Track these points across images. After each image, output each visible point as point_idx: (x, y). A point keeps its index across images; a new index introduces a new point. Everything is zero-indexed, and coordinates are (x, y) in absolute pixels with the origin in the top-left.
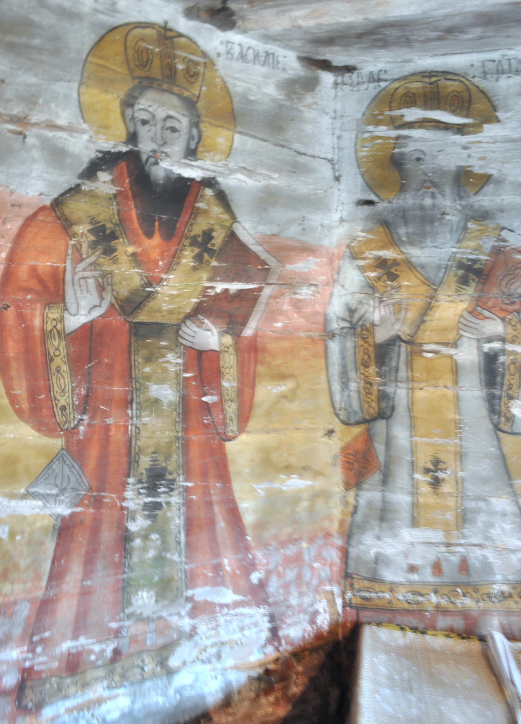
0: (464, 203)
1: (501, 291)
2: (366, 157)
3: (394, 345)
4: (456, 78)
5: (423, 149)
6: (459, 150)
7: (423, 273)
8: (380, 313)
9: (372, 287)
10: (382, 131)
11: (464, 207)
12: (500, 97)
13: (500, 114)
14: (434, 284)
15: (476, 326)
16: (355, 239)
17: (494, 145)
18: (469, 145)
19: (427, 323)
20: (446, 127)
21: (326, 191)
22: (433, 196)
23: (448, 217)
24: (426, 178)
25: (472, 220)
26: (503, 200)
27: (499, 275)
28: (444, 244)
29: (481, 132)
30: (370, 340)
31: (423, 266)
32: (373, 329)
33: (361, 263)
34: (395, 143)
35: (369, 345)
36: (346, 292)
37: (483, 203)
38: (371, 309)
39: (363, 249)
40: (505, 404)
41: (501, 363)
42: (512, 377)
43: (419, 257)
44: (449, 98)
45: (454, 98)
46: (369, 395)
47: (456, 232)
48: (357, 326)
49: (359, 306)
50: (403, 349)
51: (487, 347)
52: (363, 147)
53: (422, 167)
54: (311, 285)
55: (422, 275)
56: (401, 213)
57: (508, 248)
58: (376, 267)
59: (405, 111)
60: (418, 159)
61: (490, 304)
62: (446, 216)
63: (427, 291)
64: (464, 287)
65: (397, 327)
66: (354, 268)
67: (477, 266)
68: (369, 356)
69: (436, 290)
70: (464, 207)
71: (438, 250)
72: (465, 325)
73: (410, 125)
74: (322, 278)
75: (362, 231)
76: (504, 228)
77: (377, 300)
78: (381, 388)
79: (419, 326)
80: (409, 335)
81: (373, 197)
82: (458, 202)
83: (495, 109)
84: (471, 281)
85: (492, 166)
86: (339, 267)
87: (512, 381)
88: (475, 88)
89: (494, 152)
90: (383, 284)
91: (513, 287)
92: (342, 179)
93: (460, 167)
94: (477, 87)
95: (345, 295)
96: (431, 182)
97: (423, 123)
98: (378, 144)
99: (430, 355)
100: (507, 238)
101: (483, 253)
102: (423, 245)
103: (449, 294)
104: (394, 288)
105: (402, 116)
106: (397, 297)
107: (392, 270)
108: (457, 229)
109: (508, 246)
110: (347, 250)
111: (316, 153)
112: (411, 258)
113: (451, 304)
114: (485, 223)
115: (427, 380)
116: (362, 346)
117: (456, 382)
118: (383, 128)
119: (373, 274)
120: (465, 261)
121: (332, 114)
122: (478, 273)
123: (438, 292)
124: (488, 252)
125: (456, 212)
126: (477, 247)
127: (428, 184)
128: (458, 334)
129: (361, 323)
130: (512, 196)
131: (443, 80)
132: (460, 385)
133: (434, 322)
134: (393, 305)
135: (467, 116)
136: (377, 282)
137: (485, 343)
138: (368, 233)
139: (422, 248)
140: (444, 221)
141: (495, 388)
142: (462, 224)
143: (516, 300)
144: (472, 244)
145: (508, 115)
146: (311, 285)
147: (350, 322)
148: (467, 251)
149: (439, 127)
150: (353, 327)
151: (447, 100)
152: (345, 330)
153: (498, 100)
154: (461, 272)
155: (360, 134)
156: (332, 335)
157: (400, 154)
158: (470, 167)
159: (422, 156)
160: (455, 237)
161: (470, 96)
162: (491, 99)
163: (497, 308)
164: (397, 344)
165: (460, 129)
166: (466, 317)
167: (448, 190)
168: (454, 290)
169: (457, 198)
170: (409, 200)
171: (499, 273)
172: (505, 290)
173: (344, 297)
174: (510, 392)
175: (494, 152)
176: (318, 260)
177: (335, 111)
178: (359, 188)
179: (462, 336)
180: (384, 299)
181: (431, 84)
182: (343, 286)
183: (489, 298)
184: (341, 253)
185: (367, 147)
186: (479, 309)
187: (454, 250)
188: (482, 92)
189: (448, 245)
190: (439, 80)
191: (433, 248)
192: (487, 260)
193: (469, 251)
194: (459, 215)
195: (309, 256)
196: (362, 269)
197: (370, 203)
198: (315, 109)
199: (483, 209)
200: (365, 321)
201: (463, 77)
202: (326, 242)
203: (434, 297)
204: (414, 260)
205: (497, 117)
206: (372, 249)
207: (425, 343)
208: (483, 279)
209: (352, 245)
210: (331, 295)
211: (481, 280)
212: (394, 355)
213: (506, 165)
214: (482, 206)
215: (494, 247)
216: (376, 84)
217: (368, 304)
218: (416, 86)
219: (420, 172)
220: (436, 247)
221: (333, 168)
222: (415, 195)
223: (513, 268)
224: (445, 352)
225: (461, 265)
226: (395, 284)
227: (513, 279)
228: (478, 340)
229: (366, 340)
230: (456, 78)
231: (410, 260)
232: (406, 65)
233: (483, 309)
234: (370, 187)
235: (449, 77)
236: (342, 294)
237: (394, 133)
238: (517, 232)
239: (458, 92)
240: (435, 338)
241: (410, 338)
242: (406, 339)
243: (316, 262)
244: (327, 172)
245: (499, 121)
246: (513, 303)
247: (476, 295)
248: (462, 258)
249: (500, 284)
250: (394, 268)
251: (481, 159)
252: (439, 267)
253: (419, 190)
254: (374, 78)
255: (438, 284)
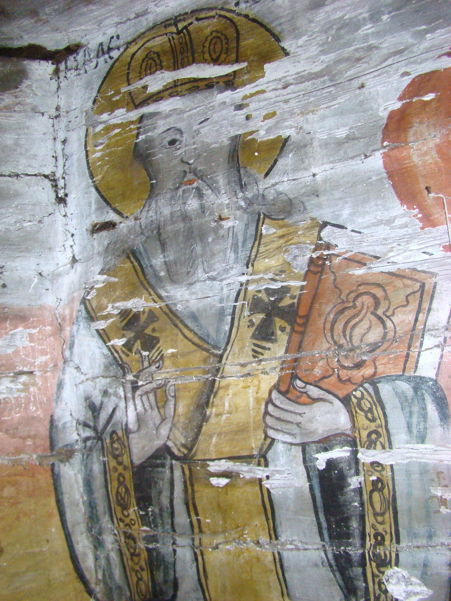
0: (249, 195)
1: (335, 343)
2: (99, 159)
3: (163, 466)
4: (213, 13)
5: (178, 126)
6: (231, 111)
7: (196, 329)
8: (136, 409)
9: (123, 367)
10: (121, 115)
11: (250, 203)
12: (283, 20)
13: (285, 44)
14: (216, 347)
15: (299, 419)
16: (92, 288)
17: (285, 92)
18: (246, 102)
19: (213, 420)
20: (208, 85)
21: (40, 222)
22: (200, 195)
23: (227, 224)
24: (186, 168)
25: (267, 220)
26: (314, 175)
27: (329, 314)
28: (226, 271)
29: (263, 77)
30: (126, 460)
31: (194, 317)
32: (128, 438)
33: (102, 325)
34: (139, 128)
35: (125, 468)
36: (83, 378)
37: (280, 188)
38: (122, 404)
39: (104, 301)
40: (374, 575)
41: (354, 490)
42: (380, 519)
43: (187, 301)
44: (207, 44)
45: (214, 41)
46: (136, 559)
47: (243, 246)
48: (104, 435)
49: (106, 400)
50: (178, 474)
51: (321, 460)
52: (96, 146)
53: (179, 152)
54: (22, 373)
55: (196, 334)
56: (155, 232)
57: (337, 261)
58: (123, 329)
59: (147, 80)
60: (172, 142)
61: (318, 372)
62: (223, 223)
63: (205, 361)
64: (269, 345)
65: (164, 431)
66: (93, 336)
67: (286, 302)
68: (127, 489)
69: (221, 357)
70: (250, 203)
71: (216, 284)
72: (278, 419)
73: (157, 97)
74: (41, 359)
75: (102, 272)
76: (325, 224)
77: (129, 386)
78: (150, 546)
79: (200, 427)
80: (184, 446)
81: (112, 216)
82: (240, 195)
83: (278, 40)
84: (279, 332)
85: (286, 124)
86: (72, 336)
87: (380, 528)
88: (243, 18)
89: (286, 102)
90: (137, 356)
91: (358, 332)
92: (69, 200)
93: (235, 139)
94: (246, 16)
95: (83, 382)
96: (194, 172)
97: (173, 90)
98: (116, 135)
99: (224, 481)
100: (333, 242)
101: (296, 278)
102: (191, 280)
103: (242, 361)
104: (155, 362)
105: (145, 87)
106: (160, 377)
107: (148, 331)
108: (245, 241)
109: (338, 256)
110: (83, 307)
111: (20, 169)
112: (175, 305)
113: (250, 379)
114: (288, 221)
115: (224, 532)
116: (116, 469)
117: (274, 534)
118: (121, 112)
119: (119, 342)
120: (263, 296)
121: (53, 113)
122: (291, 314)
123: (224, 361)
124: (303, 272)
125: (238, 213)
126: (281, 267)
127: (190, 176)
128: (266, 436)
129: (109, 429)
130: (327, 167)
131: (195, 23)
132: (282, 539)
133: (224, 417)
134: (154, 390)
135: (237, 61)
136: (128, 356)
137: (318, 452)
138: (109, 275)
139: (191, 284)
140: (222, 232)
141: (350, 544)
142: (252, 230)
143: (364, 358)
144: (273, 262)
145: (300, 42)
146: (22, 373)
147: (95, 429)
148: (265, 277)
149: (198, 87)
150: (99, 437)
151: (204, 47)
152: (89, 443)
153: (280, 24)
154: (258, 318)
155: (91, 130)
156: (68, 454)
157: (146, 141)
158: (252, 133)
159: (178, 137)
160: (243, 255)
161: (237, 31)
162: (269, 27)
163: (333, 379)
164: (168, 462)
165: (230, 83)
166: (278, 403)
167: (221, 180)
168: (251, 353)
169: (237, 188)
170: (162, 208)
171: (327, 308)
172: (342, 341)
173: (81, 387)
174: (380, 550)
175: (286, 102)
176: (34, 331)
177: (58, 109)
178: (94, 207)
179: (273, 440)
180: (140, 383)
181: (179, 32)
182: (78, 368)
183: (314, 363)
184: (75, 313)
185: (102, 144)
186: (299, 383)
187: (244, 279)
188: (254, 20)
189: (232, 272)
190: (191, 23)
191: (208, 282)
192: (302, 288)
193: (271, 276)
194: (246, 216)
195: (16, 327)
196: (104, 336)
197: (109, 226)
198: (20, 112)
199: (283, 197)
200: (116, 424)
201: (222, 9)
202: (49, 300)
203: (218, 370)
204: (179, 307)
205: (283, 49)
206: (115, 301)
207: (213, 460)
208: (299, 325)
209: (89, 297)
210: (60, 386)
211: (297, 328)
212: (164, 485)
213: (310, 116)
214: (279, 194)
215: (311, 261)
216: (107, 56)
217: (116, 394)
218: (159, 42)
219: (176, 162)
220: (213, 279)
221: (55, 186)
222: (172, 198)
223: (353, 295)
224: (248, 476)
225: (256, 305)
226: (154, 354)
227: (354, 317)
228: (304, 446)
229: (120, 459)
230: (213, 13)
231: (174, 309)
232: (143, 19)
233: (306, 383)
234: (106, 200)
235: (203, 15)
236: (78, 381)
237: (134, 115)
238: (350, 228)
239: (217, 31)
240: (227, 450)
241: (186, 452)
242: (180, 455)
243: (30, 335)
244: (44, 193)
245: (287, 54)
246: (359, 365)
247: (289, 357)
248: (259, 291)
249: (332, 330)
250: (151, 327)
251: (266, 117)
252: (221, 313)
253: (178, 188)
254: (103, 50)
255: (223, 346)
